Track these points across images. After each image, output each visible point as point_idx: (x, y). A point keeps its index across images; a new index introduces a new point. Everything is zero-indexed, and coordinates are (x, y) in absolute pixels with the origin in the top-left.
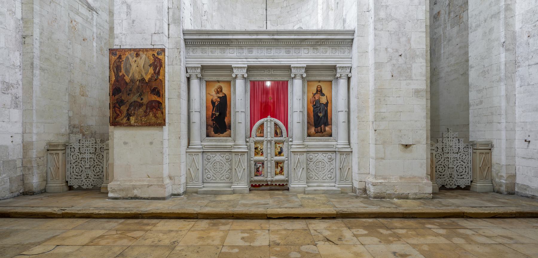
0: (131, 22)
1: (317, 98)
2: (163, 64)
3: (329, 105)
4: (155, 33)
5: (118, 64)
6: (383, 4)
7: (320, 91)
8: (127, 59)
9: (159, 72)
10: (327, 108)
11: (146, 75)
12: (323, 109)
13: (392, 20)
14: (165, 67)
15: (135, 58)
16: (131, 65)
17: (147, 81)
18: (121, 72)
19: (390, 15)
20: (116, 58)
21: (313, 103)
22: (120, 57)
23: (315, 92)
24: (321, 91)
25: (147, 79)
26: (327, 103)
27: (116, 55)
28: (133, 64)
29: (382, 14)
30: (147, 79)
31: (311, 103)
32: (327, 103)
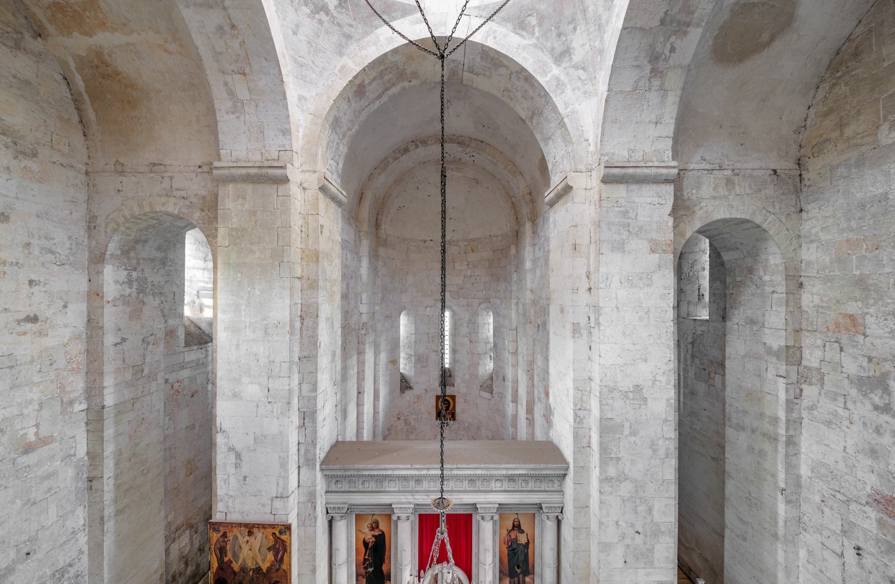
0: (242, 478)
1: (513, 537)
2: (288, 548)
3: (530, 546)
4: (276, 497)
5: (222, 544)
6: (613, 456)
7: (517, 527)
8: (236, 538)
9: (282, 558)
10: (528, 551)
11: (263, 563)
12: (522, 552)
13: (626, 479)
14: (290, 552)
15: (247, 538)
16: (240, 547)
17: (264, 571)
18: (226, 556)
19: (623, 472)
20: (219, 535)
21: (508, 543)
22: (225, 535)
23: (510, 528)
24: (519, 526)
25: (264, 568)
26: (528, 542)
27: (219, 531)
28: (244, 545)
29: (612, 471)
30: (264, 568)
31: (505, 543)
32: (528, 542)
